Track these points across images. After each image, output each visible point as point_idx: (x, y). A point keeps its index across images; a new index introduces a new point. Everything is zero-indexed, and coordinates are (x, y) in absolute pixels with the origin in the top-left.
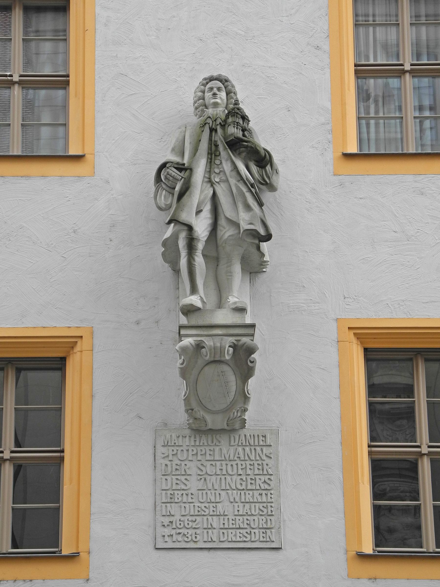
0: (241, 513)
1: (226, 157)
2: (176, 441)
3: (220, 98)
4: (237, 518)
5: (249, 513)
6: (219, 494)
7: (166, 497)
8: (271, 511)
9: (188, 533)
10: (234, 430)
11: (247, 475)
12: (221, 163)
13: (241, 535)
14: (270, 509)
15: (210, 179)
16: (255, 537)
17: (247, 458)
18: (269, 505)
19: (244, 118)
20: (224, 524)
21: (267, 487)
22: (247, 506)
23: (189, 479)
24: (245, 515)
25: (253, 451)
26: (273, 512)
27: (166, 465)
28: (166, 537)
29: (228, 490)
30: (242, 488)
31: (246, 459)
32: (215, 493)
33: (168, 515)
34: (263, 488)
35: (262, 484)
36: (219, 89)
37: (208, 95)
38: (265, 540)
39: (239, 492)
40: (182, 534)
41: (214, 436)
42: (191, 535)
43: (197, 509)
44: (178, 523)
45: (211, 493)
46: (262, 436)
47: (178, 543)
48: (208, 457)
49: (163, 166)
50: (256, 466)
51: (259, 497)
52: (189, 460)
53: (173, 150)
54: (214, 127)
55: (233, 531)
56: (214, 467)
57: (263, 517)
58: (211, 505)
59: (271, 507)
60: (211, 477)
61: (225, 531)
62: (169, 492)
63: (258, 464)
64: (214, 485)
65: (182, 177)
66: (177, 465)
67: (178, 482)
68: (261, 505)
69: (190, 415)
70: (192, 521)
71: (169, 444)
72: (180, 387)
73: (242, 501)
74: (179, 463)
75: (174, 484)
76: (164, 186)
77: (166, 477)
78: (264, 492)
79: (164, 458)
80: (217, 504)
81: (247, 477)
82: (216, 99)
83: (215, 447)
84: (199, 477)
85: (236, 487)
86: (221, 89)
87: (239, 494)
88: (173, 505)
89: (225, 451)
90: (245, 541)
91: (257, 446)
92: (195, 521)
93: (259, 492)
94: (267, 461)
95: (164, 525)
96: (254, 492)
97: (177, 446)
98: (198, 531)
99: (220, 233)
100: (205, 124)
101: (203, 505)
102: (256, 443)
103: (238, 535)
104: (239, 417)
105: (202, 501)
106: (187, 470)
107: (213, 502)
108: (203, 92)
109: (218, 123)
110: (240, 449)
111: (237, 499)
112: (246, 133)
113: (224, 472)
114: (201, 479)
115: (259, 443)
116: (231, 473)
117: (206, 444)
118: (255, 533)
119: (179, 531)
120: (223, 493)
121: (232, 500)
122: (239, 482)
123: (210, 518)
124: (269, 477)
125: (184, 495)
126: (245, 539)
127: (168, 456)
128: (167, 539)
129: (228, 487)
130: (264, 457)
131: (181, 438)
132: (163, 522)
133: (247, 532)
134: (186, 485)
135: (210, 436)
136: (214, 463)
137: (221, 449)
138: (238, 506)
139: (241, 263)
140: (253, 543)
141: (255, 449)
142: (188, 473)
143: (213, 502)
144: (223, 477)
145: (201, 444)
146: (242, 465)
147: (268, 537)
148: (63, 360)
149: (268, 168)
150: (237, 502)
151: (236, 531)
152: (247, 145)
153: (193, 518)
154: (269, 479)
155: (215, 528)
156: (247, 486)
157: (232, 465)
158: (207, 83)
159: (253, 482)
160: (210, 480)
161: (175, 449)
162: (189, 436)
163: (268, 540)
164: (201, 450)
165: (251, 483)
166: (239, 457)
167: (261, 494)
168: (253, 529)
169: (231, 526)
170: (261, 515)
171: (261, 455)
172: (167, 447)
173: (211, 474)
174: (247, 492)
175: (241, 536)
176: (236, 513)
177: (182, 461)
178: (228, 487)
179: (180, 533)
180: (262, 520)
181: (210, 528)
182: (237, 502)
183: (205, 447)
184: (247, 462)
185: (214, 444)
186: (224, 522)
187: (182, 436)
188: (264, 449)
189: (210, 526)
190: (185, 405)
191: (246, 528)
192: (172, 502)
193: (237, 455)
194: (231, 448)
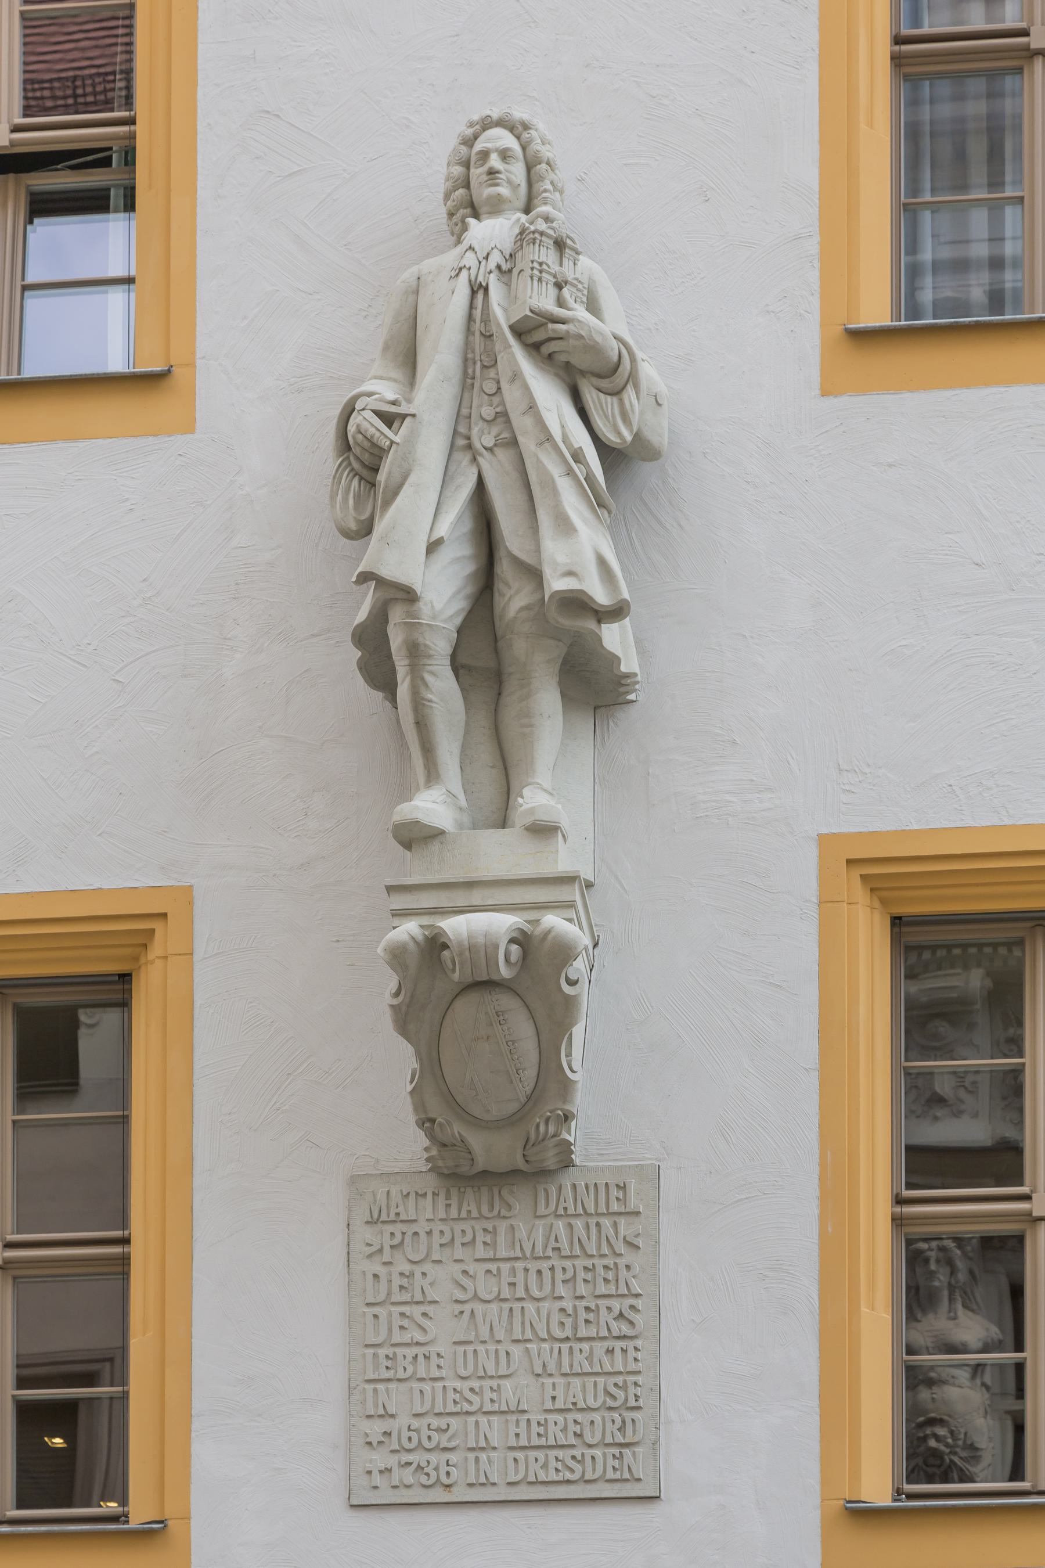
0: (559, 1404)
2: (401, 1209)
3: (509, 182)
4: (552, 1418)
5: (581, 1404)
6: (507, 1353)
7: (376, 1366)
8: (635, 1395)
9: (428, 1462)
10: (543, 1174)
11: (577, 1298)
13: (560, 1466)
14: (632, 1390)
15: (469, 438)
16: (594, 1470)
17: (577, 1251)
18: (631, 1379)
20: (517, 1435)
21: (625, 1329)
22: (577, 1382)
23: (431, 1315)
24: (570, 1410)
25: (593, 1230)
26: (641, 1400)
27: (376, 1276)
28: (375, 1474)
29: (529, 1341)
30: (563, 1336)
31: (574, 1253)
35: (612, 1321)
36: (505, 155)
37: (477, 173)
38: (618, 1476)
39: (556, 1346)
40: (414, 1466)
41: (496, 1191)
42: (436, 1469)
43: (451, 1395)
44: (405, 1434)
46: (617, 1186)
47: (405, 1492)
48: (481, 1252)
51: (606, 1359)
52: (434, 1262)
54: (480, 279)
55: (540, 1455)
56: (494, 1280)
57: (616, 1415)
58: (487, 1383)
59: (636, 1384)
60: (489, 1306)
61: (520, 1455)
62: (382, 1352)
63: (606, 1267)
64: (495, 1329)
66: (401, 1274)
67: (405, 1323)
69: (431, 1135)
70: (438, 1430)
71: (384, 1217)
72: (404, 1057)
73: (564, 1371)
74: (406, 1268)
77: (376, 1310)
78: (618, 1345)
79: (370, 1256)
80: (502, 1382)
81: (577, 1303)
82: (497, 185)
84: (459, 1307)
85: (548, 1331)
86: (509, 153)
87: (556, 1351)
88: (392, 1386)
89: (522, 1232)
90: (568, 1482)
91: (603, 1214)
92: (446, 1430)
94: (629, 1257)
95: (370, 1443)
97: (401, 1221)
98: (453, 1457)
99: (499, 602)
100: (461, 269)
102: (603, 1209)
103: (553, 1464)
104: (554, 1136)
105: (464, 1373)
106: (428, 1289)
107: (492, 1377)
108: (467, 164)
109: (492, 264)
111: (552, 1367)
113: (521, 1293)
114: (462, 1312)
115: (608, 1208)
116: (536, 1294)
119: (406, 1458)
120: (516, 1351)
121: (539, 1370)
122: (556, 1317)
123: (483, 1420)
125: (421, 1358)
126: (568, 1476)
127: (380, 1251)
128: (377, 1479)
129: (529, 1335)
130: (621, 1248)
131: (413, 1196)
132: (367, 1435)
133: (573, 1457)
134: (424, 1330)
135: (484, 1190)
136: (493, 1267)
137: (512, 1228)
138: (554, 1384)
139: (560, 683)
140: (589, 1486)
141: (598, 1224)
142: (429, 1299)
143: (492, 1377)
144: (517, 1306)
145: (464, 1215)
147: (626, 1469)
148: (125, 978)
150: (551, 1375)
151: (547, 1455)
153: (442, 1423)
155: (494, 1448)
156: (575, 1328)
157: (539, 1272)
158: (476, 137)
160: (484, 1315)
162: (434, 1194)
163: (626, 1475)
165: (587, 1321)
166: (559, 1249)
167: (610, 1352)
168: (590, 1446)
169: (535, 1441)
170: (610, 1409)
171: (613, 1240)
172: (380, 1225)
173: (488, 1297)
174: (576, 1346)
175: (560, 1468)
176: (549, 1405)
177: (415, 1263)
178: (529, 1335)
180: (613, 1421)
181: (483, 1449)
182: (551, 1375)
183: (473, 1222)
184: (577, 1262)
185: (496, 1212)
186: (518, 1431)
187: (417, 1193)
188: (622, 1221)
189: (482, 1444)
191: (573, 1446)
192: (389, 1380)
194: (537, 1222)
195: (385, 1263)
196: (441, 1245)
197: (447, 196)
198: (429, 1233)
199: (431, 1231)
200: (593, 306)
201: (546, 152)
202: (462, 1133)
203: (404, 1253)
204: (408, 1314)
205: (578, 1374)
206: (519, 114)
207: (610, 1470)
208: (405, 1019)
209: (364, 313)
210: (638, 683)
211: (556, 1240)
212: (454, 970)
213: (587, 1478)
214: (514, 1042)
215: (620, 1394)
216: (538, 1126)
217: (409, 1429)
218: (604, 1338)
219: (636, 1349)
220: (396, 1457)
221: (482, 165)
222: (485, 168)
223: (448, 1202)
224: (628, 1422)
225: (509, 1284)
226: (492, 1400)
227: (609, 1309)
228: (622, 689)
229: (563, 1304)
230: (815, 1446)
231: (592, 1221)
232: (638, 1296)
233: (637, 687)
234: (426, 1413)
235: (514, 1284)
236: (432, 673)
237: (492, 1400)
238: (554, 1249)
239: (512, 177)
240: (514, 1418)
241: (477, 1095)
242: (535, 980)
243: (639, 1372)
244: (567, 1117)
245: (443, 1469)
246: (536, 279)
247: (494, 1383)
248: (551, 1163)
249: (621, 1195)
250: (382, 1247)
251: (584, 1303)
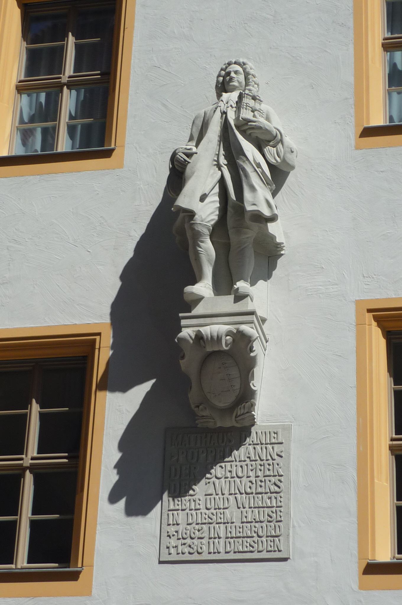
3: (238, 81)
4: (245, 524)
5: (258, 520)
21: (277, 489)
22: (256, 510)
34: (272, 490)
36: (236, 72)
39: (248, 496)
51: (268, 501)
55: (240, 540)
59: (280, 512)
61: (232, 540)
80: (224, 510)
90: (252, 552)
96: (263, 495)
110: (251, 447)
114: (209, 483)
119: (185, 541)
120: (232, 498)
124: (280, 478)
130: (276, 457)
146: (252, 465)
158: (226, 68)
169: (239, 535)
174: (256, 496)
179: (184, 544)
188: (275, 446)
200: (268, 119)
201: (252, 72)
206: (241, 60)
207: (269, 546)
219: (281, 497)
227: (270, 481)
228: (278, 249)
229: (251, 479)
230: (355, 537)
231: (264, 446)
232: (282, 476)
233: (284, 248)
239: (239, 80)
247: (222, 511)
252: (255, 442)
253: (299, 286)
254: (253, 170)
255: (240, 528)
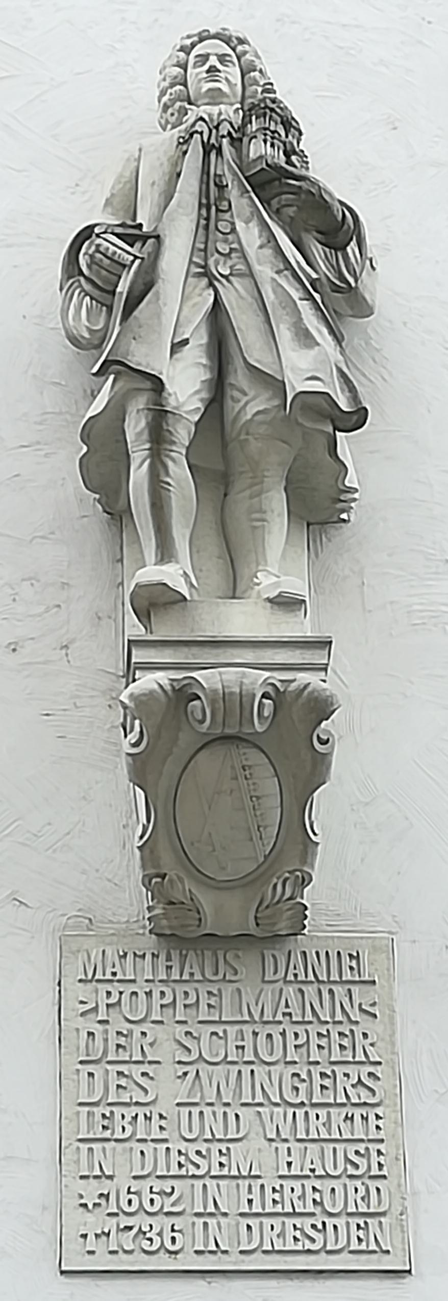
1: (247, 211)
2: (117, 969)
6: (237, 1116)
8: (379, 1163)
9: (151, 1226)
11: (310, 1063)
12: (233, 230)
13: (298, 1234)
17: (309, 1017)
18: (373, 1147)
19: (288, 123)
20: (250, 1201)
21: (365, 1096)
24: (308, 1177)
25: (326, 996)
26: (385, 1168)
27: (90, 1034)
28: (91, 1237)
32: (225, 1113)
33: (96, 1177)
34: (355, 1100)
36: (222, 58)
38: (363, 1247)
39: (290, 1111)
40: (135, 1230)
43: (175, 1158)
45: (214, 1113)
49: (87, 233)
50: (335, 1036)
53: (108, 203)
55: (277, 1222)
56: (222, 1042)
57: (358, 1183)
59: (379, 1152)
61: (254, 1222)
65: (136, 257)
66: (118, 1033)
67: (123, 1082)
68: (352, 1148)
70: (161, 1193)
73: (298, 1137)
74: (125, 1027)
75: (112, 1088)
76: (87, 287)
77: (90, 1068)
78: (358, 1112)
79: (83, 1014)
80: (230, 1146)
81: (312, 1068)
83: (222, 986)
84: (181, 1070)
89: (248, 997)
90: (309, 1251)
93: (344, 1111)
94: (366, 1024)
95: (85, 1206)
96: (331, 1110)
97: (119, 981)
98: (179, 1223)
99: (231, 408)
100: (191, 135)
101: (192, 1148)
103: (290, 1232)
107: (220, 1140)
110: (290, 991)
112: (294, 158)
117: (198, 977)
118: (335, 1227)
119: (125, 1221)
123: (211, 1184)
124: (371, 1069)
125: (141, 1118)
126: (309, 1245)
127: (95, 1009)
129: (259, 1099)
130: (355, 1015)
131: (130, 957)
132: (81, 1197)
133: (314, 1226)
136: (220, 1030)
138: (289, 1149)
141: (331, 992)
142: (150, 1058)
143: (220, 1140)
144: (246, 1070)
146: (296, 1035)
149: (352, 249)
150: (286, 1140)
151: (284, 1223)
152: (300, 187)
153: (167, 1186)
154: (370, 1074)
155: (225, 1215)
157: (269, 1036)
158: (193, 45)
159: (327, 1082)
161: (114, 988)
162: (153, 954)
163: (373, 1247)
164: (186, 993)
165: (323, 1087)
166: (290, 1014)
167: (349, 1119)
168: (331, 1215)
171: (347, 1008)
180: (356, 1190)
181: (211, 1215)
182: (286, 1140)
183: (196, 985)
185: (221, 976)
187: (135, 954)
188: (355, 989)
189: (211, 1209)
190: (143, 867)
191: (313, 1214)
193: (282, 1009)
194: (266, 986)
195: (100, 1022)
196: (162, 1006)
197: (163, 93)
198: (149, 994)
199: (151, 991)
202: (193, 890)
203: (121, 1012)
204: (126, 1073)
205: (313, 1141)
206: (235, 30)
208: (141, 770)
209: (72, 190)
210: (355, 500)
211: (287, 1006)
212: (202, 722)
213: (329, 1248)
214: (258, 798)
215: (362, 1162)
216: (275, 886)
217: (129, 1192)
218: (343, 1105)
219: (378, 1117)
220: (114, 1220)
221: (204, 64)
222: (206, 67)
223: (169, 964)
224: (373, 1192)
225: (237, 1047)
226: (221, 1164)
227: (347, 1075)
234: (148, 1176)
235: (243, 1047)
236: (173, 460)
237: (221, 1164)
238: (284, 1014)
240: (247, 1182)
241: (214, 850)
242: (289, 735)
243: (382, 1141)
244: (305, 880)
245: (167, 1235)
246: (269, 144)
248: (283, 927)
249: (354, 963)
250: (97, 1005)
251: (319, 1068)
252: (301, 977)
253: (392, 603)
254: (301, 294)
255: (274, 1190)
